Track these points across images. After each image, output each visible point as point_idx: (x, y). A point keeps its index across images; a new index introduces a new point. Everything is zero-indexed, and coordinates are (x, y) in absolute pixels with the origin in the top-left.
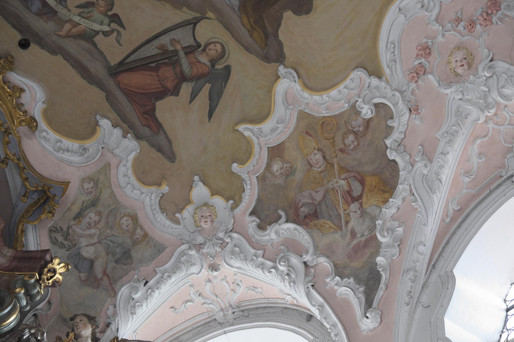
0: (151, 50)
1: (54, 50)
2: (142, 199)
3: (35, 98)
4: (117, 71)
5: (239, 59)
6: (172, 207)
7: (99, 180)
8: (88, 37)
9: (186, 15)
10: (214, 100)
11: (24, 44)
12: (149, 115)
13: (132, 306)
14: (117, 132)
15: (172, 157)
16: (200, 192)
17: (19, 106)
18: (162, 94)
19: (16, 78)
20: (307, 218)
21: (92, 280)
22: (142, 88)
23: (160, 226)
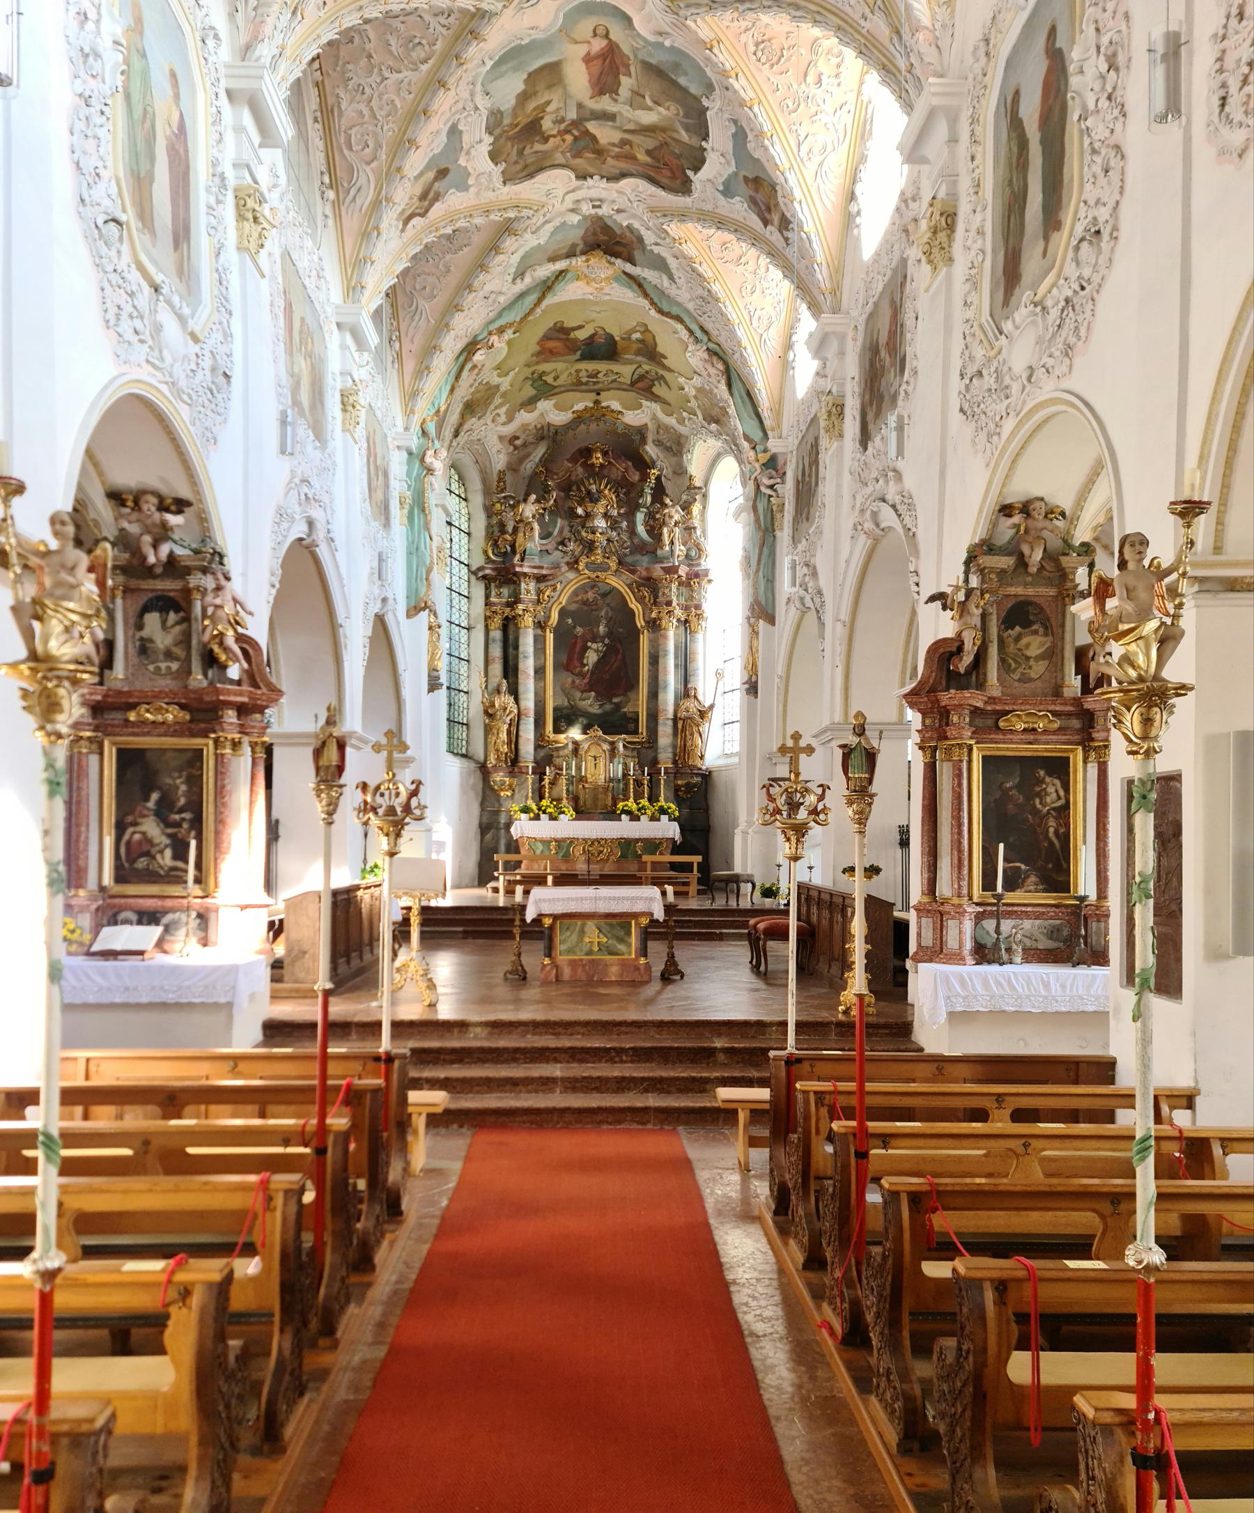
0: (636, 377)
1: (609, 390)
2: (671, 421)
3: (615, 405)
4: (633, 384)
5: (661, 372)
6: (681, 421)
7: (654, 418)
8: (615, 381)
9: (635, 366)
10: (666, 383)
11: (598, 394)
12: (652, 393)
13: (690, 461)
14: (648, 403)
15: (669, 404)
16: (685, 414)
17: (613, 411)
18: (651, 387)
19: (604, 404)
20: (717, 422)
21: (675, 455)
22: (644, 387)
23: (682, 429)
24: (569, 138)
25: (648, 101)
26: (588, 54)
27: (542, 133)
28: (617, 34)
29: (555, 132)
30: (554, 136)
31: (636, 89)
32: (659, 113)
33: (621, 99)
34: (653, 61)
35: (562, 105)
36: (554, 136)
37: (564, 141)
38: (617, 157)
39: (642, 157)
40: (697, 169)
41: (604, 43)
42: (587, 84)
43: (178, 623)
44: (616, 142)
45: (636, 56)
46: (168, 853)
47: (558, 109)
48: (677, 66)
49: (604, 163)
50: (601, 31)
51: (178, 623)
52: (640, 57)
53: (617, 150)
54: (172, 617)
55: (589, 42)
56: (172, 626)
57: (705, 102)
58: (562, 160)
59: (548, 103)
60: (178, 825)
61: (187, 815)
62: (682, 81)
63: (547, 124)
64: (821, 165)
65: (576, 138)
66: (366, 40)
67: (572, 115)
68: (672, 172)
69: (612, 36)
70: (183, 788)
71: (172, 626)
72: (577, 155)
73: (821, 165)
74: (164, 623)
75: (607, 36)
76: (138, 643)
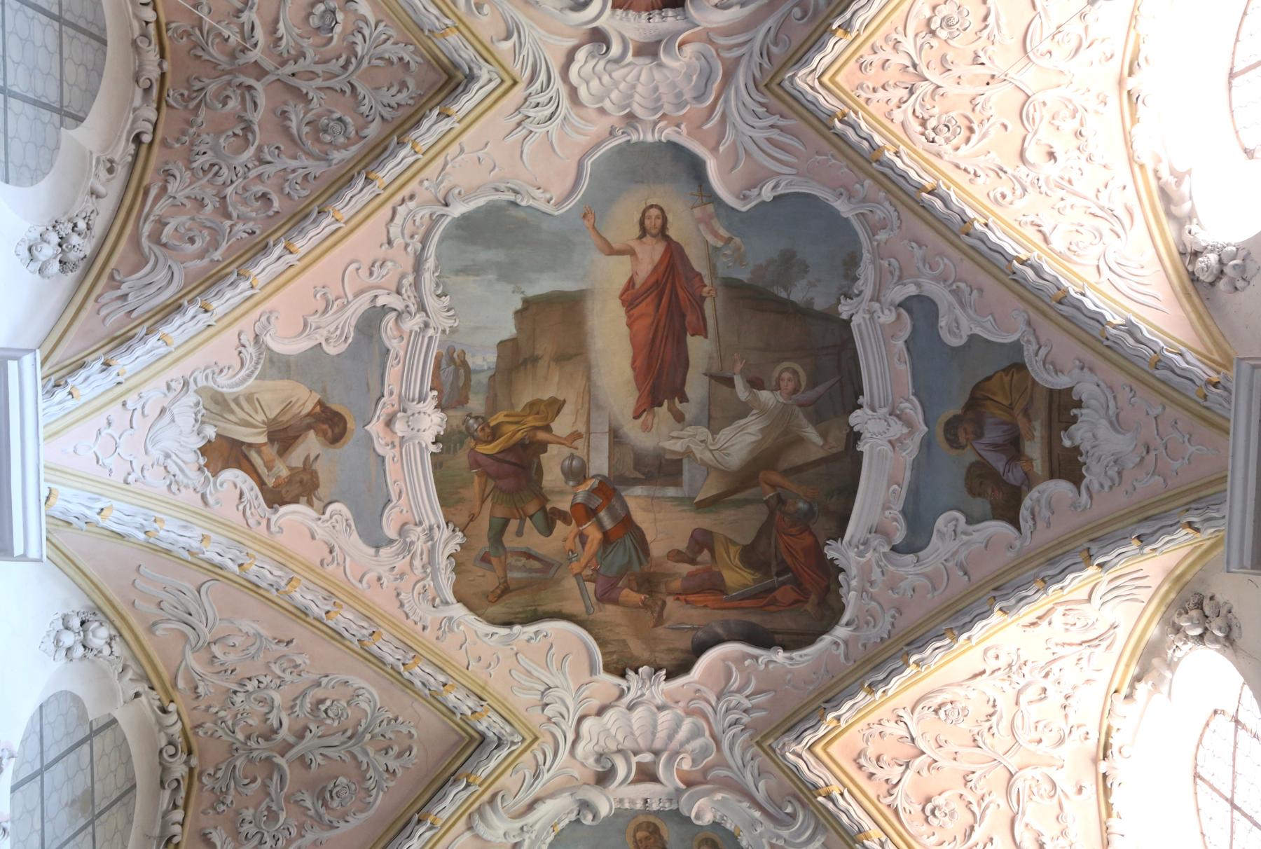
24: (594, 535)
25: (741, 391)
26: (631, 282)
27: (542, 498)
28: (684, 225)
29: (565, 506)
30: (564, 517)
31: (713, 371)
32: (763, 411)
33: (690, 410)
34: (744, 275)
35: (582, 429)
36: (564, 517)
37: (583, 538)
38: (682, 595)
39: (736, 577)
40: (840, 533)
41: (659, 249)
42: (629, 373)
44: (682, 545)
45: (713, 269)
47: (576, 436)
48: (788, 264)
49: (659, 621)
50: (653, 222)
52: (721, 272)
53: (685, 568)
55: (631, 252)
57: (844, 310)
58: (577, 608)
59: (556, 406)
62: (798, 294)
63: (552, 476)
65: (607, 540)
66: (249, 105)
67: (600, 464)
68: (798, 583)
69: (672, 233)
72: (607, 596)
75: (663, 233)
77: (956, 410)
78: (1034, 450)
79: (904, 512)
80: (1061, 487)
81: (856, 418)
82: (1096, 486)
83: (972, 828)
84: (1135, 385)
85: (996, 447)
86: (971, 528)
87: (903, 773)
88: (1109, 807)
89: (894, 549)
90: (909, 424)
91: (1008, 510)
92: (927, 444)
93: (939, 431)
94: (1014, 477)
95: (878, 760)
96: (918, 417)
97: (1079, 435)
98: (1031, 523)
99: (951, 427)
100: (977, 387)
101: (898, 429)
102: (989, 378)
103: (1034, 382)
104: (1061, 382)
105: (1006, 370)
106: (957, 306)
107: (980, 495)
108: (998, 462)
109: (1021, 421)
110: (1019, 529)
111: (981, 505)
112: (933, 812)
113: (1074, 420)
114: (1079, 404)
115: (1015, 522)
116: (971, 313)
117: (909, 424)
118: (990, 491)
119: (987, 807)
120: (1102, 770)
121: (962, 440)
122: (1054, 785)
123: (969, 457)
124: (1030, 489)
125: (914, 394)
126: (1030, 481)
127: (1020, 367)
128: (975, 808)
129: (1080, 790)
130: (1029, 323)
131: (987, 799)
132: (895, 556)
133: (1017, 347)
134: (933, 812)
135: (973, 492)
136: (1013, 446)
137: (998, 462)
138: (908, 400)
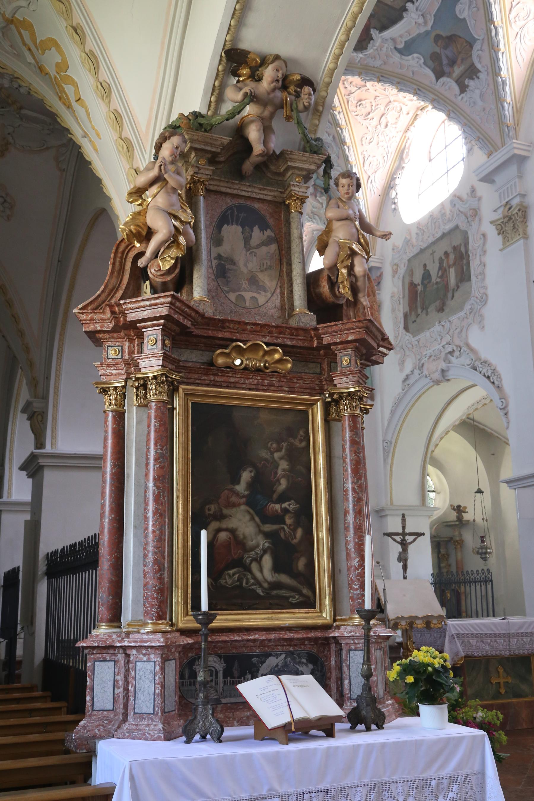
43: (264, 243)
46: (267, 561)
51: (264, 243)
54: (257, 235)
56: (258, 246)
60: (279, 519)
61: (291, 505)
64: (522, 28)
70: (284, 465)
71: (258, 246)
73: (522, 28)
74: (247, 240)
76: (215, 263)
77: (444, 34)
78: (457, 71)
79: (406, 42)
80: (456, 88)
81: (409, 5)
82: (465, 100)
83: (369, 113)
84: (494, 94)
85: (447, 57)
86: (423, 66)
87: (357, 90)
88: (413, 123)
89: (395, 48)
90: (426, 23)
91: (439, 74)
92: (427, 33)
93: (433, 35)
94: (446, 69)
95: (351, 83)
96: (430, 23)
97: (472, 83)
98: (442, 84)
99: (438, 37)
100: (455, 35)
101: (421, 20)
102: (460, 37)
103: (471, 55)
104: (479, 66)
105: (467, 42)
106: (468, 6)
107: (433, 61)
108: (445, 62)
109: (459, 61)
110: (437, 81)
111: (430, 63)
112: (360, 105)
113: (473, 79)
114: (478, 78)
115: (437, 79)
116: (470, 13)
117: (426, 23)
118: (436, 64)
119: (377, 109)
120: (418, 113)
121: (439, 43)
122: (401, 109)
123: (437, 50)
124: (448, 77)
125: (434, 16)
126: (449, 75)
127: (471, 47)
128: (373, 108)
129: (408, 114)
130: (483, 39)
131: (379, 106)
132: (394, 51)
133: (475, 40)
134: (360, 105)
135: (431, 58)
136: (452, 63)
137: (445, 62)
138: (430, 15)
